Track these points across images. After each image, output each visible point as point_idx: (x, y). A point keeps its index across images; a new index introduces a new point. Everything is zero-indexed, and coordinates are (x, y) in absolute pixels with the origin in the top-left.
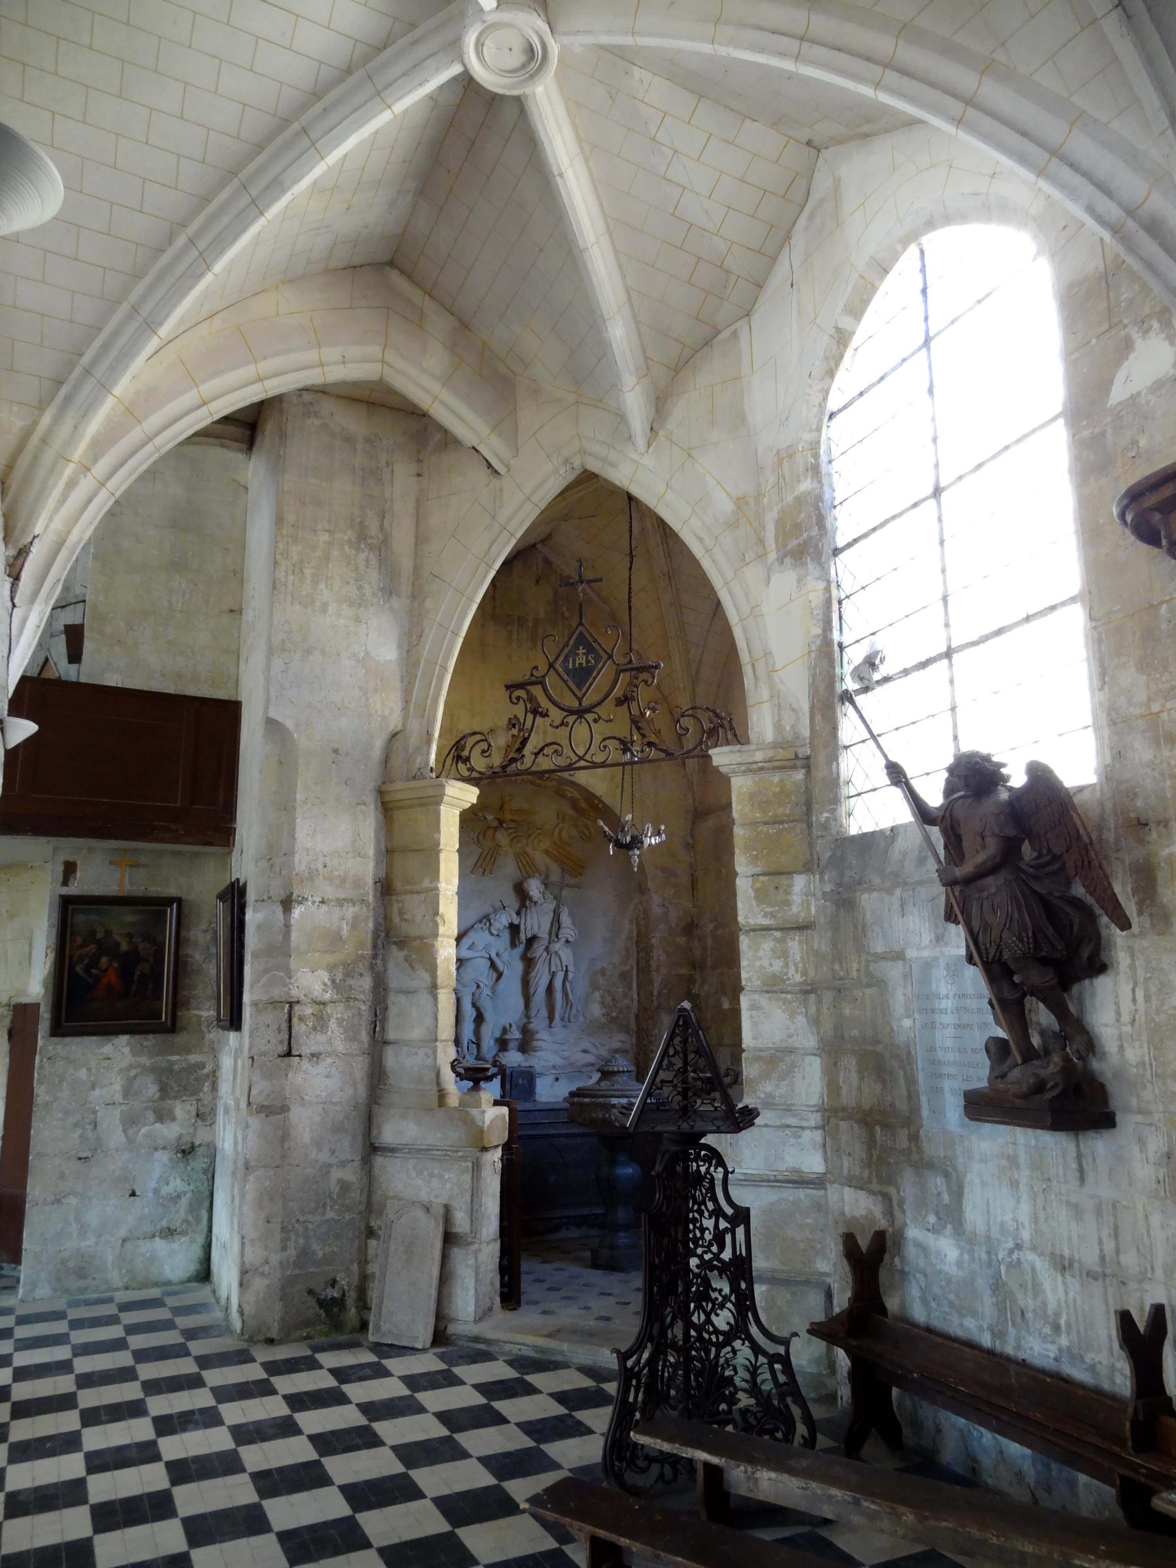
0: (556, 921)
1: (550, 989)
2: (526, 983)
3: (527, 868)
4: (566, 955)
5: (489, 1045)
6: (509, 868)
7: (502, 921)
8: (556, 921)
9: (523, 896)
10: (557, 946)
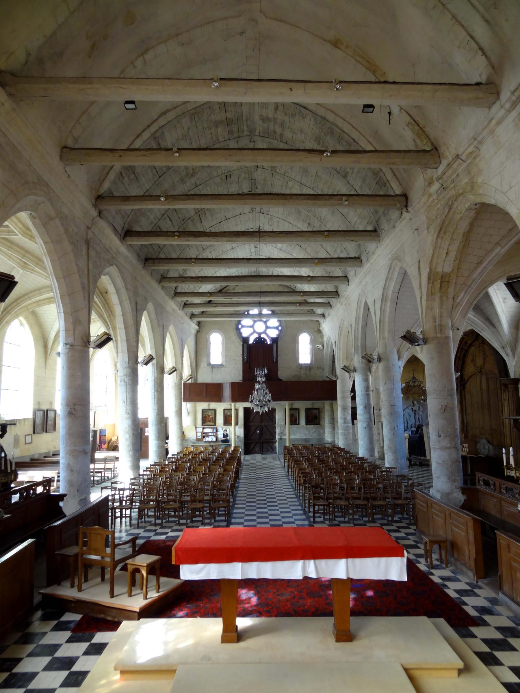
0: (419, 407)
1: (419, 418)
2: (415, 417)
3: (414, 399)
4: (421, 413)
5: (409, 426)
6: (411, 399)
7: (410, 408)
8: (419, 407)
9: (414, 404)
10: (420, 412)
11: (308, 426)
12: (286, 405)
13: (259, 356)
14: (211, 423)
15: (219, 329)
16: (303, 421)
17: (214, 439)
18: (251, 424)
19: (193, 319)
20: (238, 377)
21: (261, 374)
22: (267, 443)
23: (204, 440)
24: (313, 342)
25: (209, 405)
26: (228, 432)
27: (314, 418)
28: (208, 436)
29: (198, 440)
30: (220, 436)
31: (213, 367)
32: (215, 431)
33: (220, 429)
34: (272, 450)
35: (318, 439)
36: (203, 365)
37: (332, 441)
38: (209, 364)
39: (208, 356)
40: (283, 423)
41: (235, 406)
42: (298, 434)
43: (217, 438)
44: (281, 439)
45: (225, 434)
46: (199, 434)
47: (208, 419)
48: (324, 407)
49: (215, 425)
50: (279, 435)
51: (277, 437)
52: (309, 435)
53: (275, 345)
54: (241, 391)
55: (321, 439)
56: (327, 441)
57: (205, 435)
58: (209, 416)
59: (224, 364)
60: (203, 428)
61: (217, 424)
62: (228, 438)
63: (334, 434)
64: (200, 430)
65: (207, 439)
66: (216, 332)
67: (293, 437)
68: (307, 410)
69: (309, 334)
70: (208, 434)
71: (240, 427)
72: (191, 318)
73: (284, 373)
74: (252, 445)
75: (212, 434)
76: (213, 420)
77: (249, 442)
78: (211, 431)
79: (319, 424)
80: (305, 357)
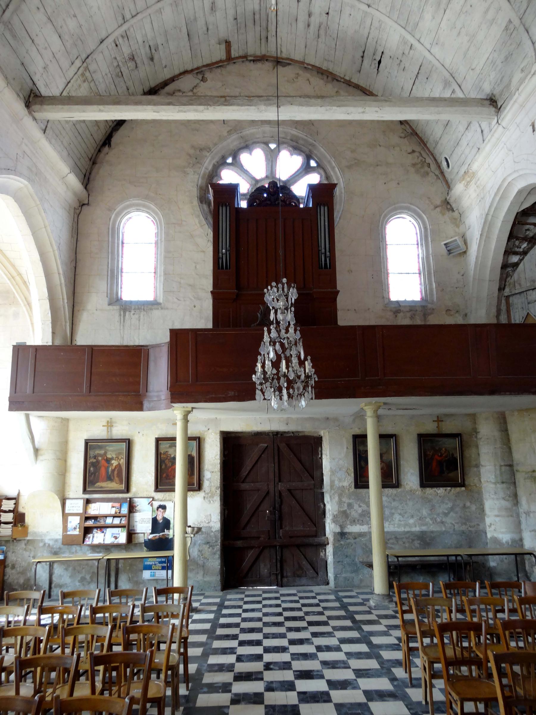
11: (429, 491)
12: (366, 413)
13: (273, 251)
14: (113, 485)
15: (147, 198)
16: (410, 476)
17: (122, 538)
18: (245, 486)
19: (36, 107)
20: (198, 314)
21: (279, 300)
22: (298, 546)
23: (88, 541)
24: (427, 237)
25: (110, 424)
26: (168, 514)
27: (444, 464)
28: (102, 528)
29: (69, 541)
30: (143, 526)
31: (126, 308)
32: (125, 510)
33: (142, 504)
34: (316, 570)
35: (463, 532)
36: (95, 303)
37: (513, 541)
38: (115, 300)
39: (114, 275)
40: (348, 481)
41: (186, 420)
42: (397, 517)
43: (131, 535)
44: (342, 535)
45: (160, 518)
46: (74, 522)
47: (104, 468)
48: (475, 431)
49: (128, 490)
50: (335, 520)
51: (330, 528)
52: (434, 520)
53: (324, 210)
54: (211, 363)
55: (474, 535)
56: (495, 540)
57: (90, 523)
58: (108, 461)
59: (161, 301)
60: (88, 502)
61: (134, 488)
62: (169, 533)
63: (518, 516)
64: (75, 506)
65: (97, 538)
66: (138, 208)
67: (389, 527)
68: (425, 440)
69: (417, 216)
70: (102, 523)
71: (208, 498)
72: (28, 105)
73: (352, 310)
74: (250, 555)
75: (117, 521)
76: (120, 475)
77: (239, 543)
78: (113, 511)
79: (463, 485)
80: (405, 279)
